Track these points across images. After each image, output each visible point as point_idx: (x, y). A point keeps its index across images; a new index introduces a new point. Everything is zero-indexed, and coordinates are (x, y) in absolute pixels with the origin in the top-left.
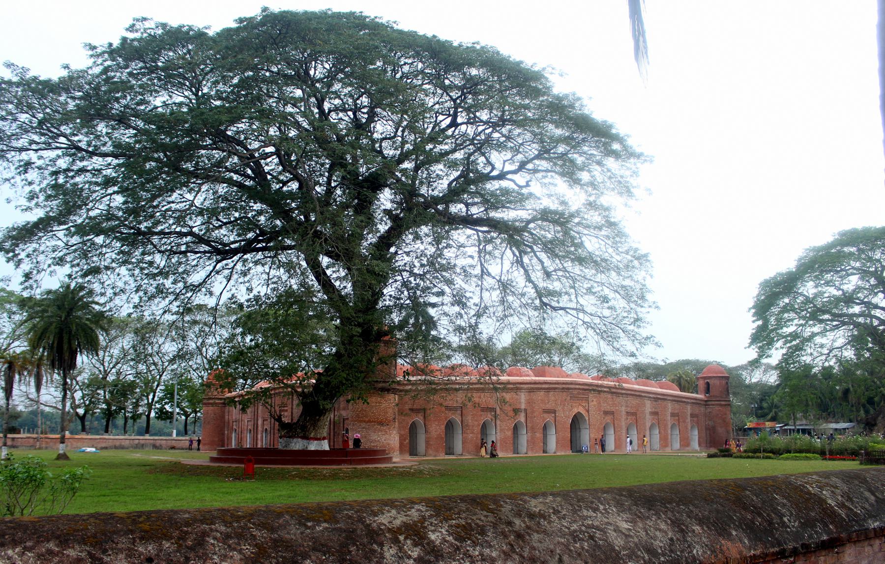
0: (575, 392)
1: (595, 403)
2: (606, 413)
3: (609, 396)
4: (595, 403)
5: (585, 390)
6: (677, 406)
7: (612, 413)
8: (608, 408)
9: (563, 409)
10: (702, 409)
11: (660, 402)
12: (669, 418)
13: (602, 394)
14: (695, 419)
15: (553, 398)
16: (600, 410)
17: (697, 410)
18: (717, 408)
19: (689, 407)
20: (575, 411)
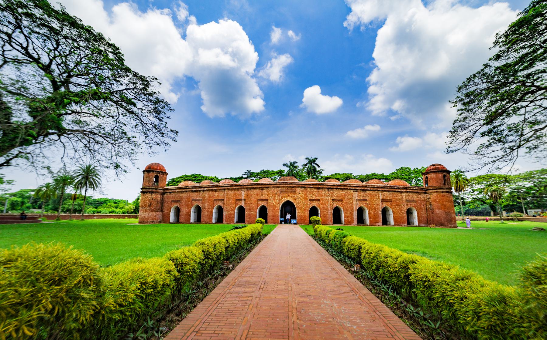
0: (284, 189)
1: (301, 194)
2: (311, 200)
3: (315, 190)
4: (301, 194)
5: (293, 187)
6: (388, 194)
7: (319, 200)
8: (314, 197)
9: (274, 200)
10: (422, 196)
11: (368, 192)
12: (380, 203)
13: (309, 190)
14: (413, 204)
15: (266, 193)
16: (306, 199)
17: (414, 197)
18: (435, 195)
19: (404, 195)
20: (285, 200)
